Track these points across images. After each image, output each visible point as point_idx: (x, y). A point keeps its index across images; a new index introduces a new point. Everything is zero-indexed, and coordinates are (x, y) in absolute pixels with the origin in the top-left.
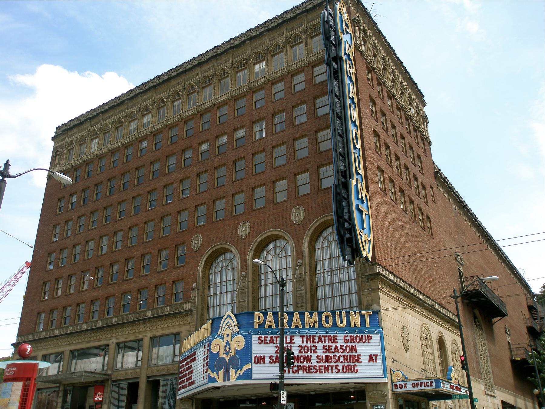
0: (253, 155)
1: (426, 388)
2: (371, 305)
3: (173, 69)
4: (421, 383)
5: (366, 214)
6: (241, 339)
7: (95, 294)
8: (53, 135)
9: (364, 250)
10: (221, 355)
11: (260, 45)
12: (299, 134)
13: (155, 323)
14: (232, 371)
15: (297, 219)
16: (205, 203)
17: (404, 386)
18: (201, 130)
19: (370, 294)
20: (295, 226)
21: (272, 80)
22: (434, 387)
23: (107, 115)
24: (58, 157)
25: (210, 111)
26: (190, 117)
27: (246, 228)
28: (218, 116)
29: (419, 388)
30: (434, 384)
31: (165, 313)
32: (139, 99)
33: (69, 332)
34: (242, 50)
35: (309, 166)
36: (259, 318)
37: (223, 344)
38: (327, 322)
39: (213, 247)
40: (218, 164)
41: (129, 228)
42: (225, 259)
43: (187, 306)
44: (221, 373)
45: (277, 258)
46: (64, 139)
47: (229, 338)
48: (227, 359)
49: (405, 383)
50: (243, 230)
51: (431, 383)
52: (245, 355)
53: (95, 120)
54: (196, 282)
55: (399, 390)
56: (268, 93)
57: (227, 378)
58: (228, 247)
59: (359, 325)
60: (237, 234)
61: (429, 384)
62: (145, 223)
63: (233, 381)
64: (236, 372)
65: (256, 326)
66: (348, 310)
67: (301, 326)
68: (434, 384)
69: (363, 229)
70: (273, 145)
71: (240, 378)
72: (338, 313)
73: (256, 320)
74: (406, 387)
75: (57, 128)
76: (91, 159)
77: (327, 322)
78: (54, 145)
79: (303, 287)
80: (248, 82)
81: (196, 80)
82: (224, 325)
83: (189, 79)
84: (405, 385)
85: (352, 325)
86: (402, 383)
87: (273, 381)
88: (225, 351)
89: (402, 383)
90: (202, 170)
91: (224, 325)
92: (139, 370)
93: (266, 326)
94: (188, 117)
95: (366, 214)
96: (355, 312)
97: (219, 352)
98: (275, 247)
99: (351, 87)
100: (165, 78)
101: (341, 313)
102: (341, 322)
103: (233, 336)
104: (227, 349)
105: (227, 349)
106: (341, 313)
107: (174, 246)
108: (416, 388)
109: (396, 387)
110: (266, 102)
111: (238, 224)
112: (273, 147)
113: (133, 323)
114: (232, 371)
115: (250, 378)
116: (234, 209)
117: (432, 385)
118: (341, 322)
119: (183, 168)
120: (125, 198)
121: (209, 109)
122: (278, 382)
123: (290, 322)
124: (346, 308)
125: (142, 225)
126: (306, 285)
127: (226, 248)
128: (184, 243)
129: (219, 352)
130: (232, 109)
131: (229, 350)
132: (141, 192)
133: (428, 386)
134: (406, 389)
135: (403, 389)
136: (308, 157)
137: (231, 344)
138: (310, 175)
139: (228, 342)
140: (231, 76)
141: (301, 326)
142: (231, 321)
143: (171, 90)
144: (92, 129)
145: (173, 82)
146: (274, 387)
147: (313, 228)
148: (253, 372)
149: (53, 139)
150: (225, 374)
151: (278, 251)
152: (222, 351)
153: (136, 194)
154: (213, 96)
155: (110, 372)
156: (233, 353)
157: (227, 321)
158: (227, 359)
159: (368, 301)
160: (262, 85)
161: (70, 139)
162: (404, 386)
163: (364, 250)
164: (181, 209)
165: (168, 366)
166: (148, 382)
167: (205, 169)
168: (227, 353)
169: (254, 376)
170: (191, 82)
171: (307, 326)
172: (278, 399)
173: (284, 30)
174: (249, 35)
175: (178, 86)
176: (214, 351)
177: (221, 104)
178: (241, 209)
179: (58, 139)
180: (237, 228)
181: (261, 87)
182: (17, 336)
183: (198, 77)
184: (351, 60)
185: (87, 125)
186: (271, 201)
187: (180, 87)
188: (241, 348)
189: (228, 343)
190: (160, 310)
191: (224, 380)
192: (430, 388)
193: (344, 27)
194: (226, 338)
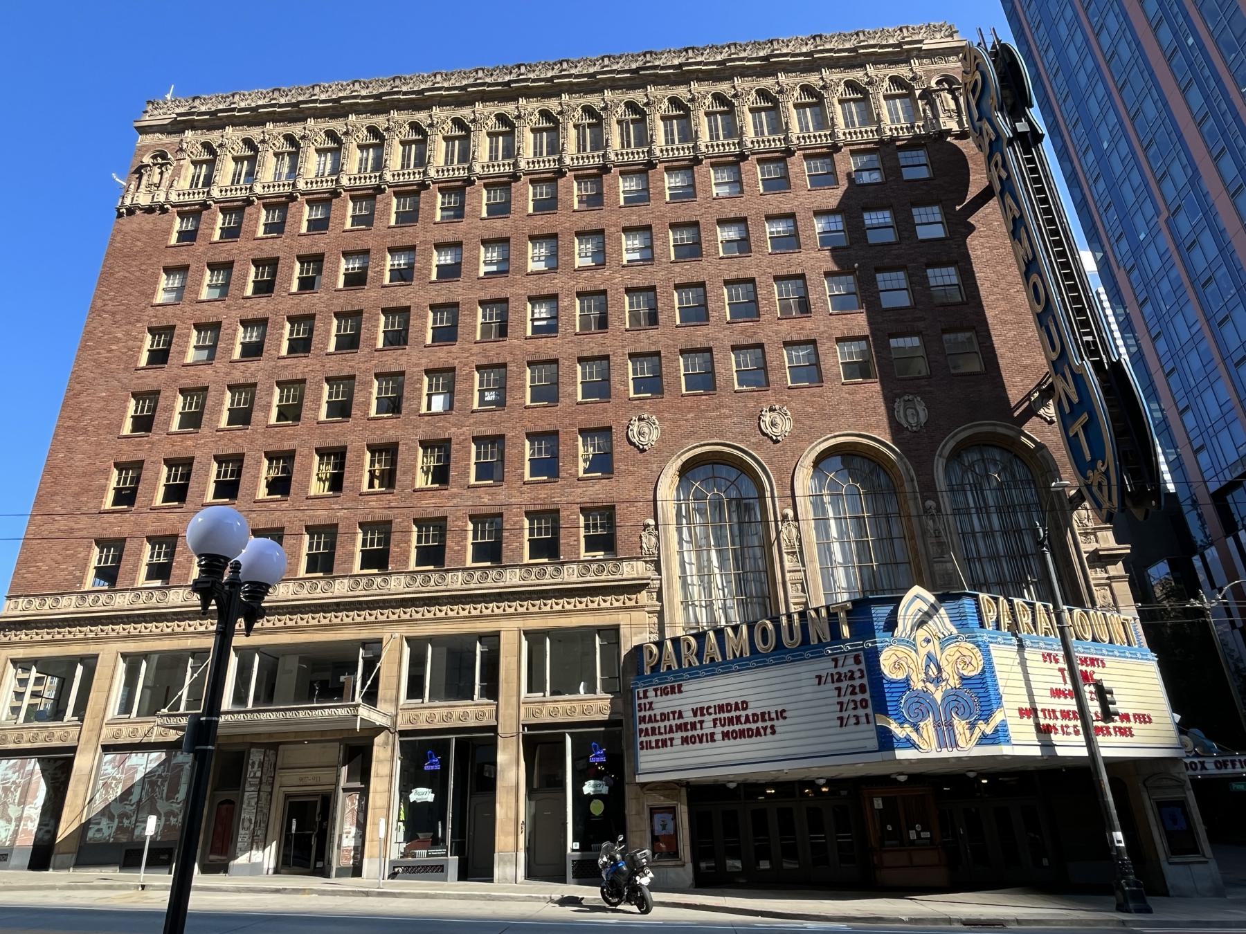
10: (918, 685)
14: (960, 725)
17: (1199, 766)
44: (928, 726)
48: (938, 696)
55: (1191, 772)
64: (972, 726)
71: (984, 740)
74: (1203, 768)
84: (1202, 763)
86: (1196, 760)
89: (1196, 760)
108: (1223, 771)
114: (960, 725)
115: (1008, 742)
139: (929, 657)
147: (952, 444)
148: (1011, 728)
156: (954, 682)
158: (938, 696)
169: (1014, 737)
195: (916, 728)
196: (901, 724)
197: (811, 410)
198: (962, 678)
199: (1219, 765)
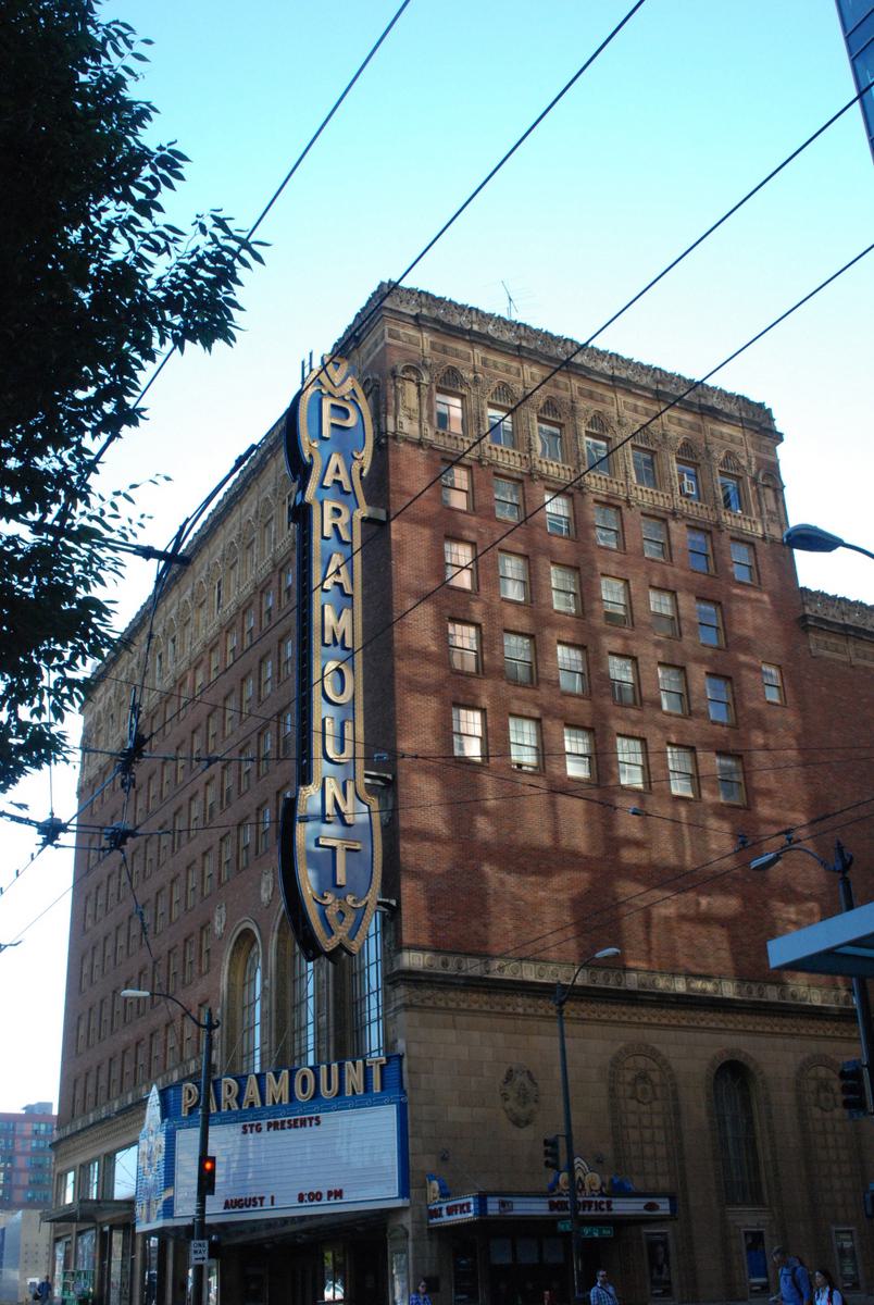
30: (472, 1207)
51: (468, 1204)
65: (185, 1114)
67: (258, 1105)
73: (185, 1094)
85: (348, 1093)
99: (337, 560)
102: (329, 1088)
108: (451, 1218)
141: (258, 1105)
148: (177, 1203)
163: (331, 932)
164: (205, 849)
171: (269, 1103)
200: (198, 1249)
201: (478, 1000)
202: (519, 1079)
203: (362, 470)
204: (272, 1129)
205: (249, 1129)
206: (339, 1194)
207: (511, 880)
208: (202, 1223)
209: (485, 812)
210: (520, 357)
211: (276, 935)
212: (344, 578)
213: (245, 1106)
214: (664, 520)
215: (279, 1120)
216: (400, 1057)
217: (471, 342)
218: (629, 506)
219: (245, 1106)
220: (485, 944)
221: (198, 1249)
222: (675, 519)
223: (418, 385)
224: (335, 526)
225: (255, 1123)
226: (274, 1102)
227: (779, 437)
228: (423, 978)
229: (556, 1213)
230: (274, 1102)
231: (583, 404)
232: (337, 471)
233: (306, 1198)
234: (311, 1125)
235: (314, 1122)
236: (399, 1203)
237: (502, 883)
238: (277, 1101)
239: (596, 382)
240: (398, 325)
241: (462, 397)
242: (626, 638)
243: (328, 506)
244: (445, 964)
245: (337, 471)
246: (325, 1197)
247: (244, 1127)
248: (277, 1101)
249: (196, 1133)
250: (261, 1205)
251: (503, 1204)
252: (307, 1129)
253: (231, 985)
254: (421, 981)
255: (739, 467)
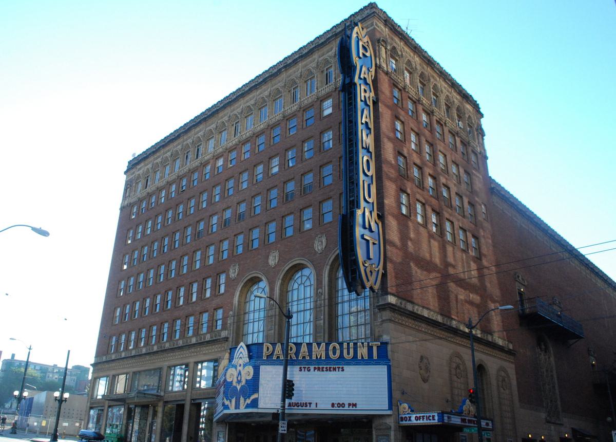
0: (284, 183)
1: (429, 421)
2: (382, 336)
3: (222, 100)
4: (423, 417)
5: (374, 244)
6: (251, 369)
7: (153, 320)
8: (125, 169)
9: (368, 280)
10: (234, 384)
11: (295, 72)
12: (325, 161)
13: (198, 349)
14: (242, 399)
15: (319, 248)
16: (242, 232)
17: (408, 419)
18: (242, 159)
19: (381, 324)
20: (318, 255)
21: (303, 107)
22: (436, 421)
23: (167, 149)
24: (128, 189)
25: (250, 140)
26: (233, 148)
27: (275, 257)
28: (257, 145)
29: (421, 422)
31: (207, 340)
32: (193, 132)
33: (132, 355)
34: (279, 78)
35: (332, 193)
36: (268, 348)
37: (236, 374)
38: (334, 353)
39: (248, 276)
40: (255, 193)
41: (181, 257)
42: (258, 288)
43: (224, 334)
45: (303, 286)
46: (134, 172)
47: (241, 368)
48: (239, 387)
49: (409, 415)
50: (273, 261)
51: (433, 416)
52: (253, 385)
53: (158, 154)
54: (232, 311)
56: (299, 120)
57: (237, 406)
58: (260, 276)
59: (366, 357)
60: (268, 263)
61: (431, 418)
62: (194, 252)
63: (242, 410)
64: (245, 400)
65: (265, 358)
66: (355, 341)
68: (436, 418)
69: (369, 258)
70: (302, 173)
71: (247, 406)
72: (345, 345)
73: (265, 349)
74: (410, 420)
75: (129, 162)
76: (153, 191)
77: (334, 353)
78: (126, 178)
79: (322, 317)
80: (283, 110)
81: (239, 110)
82: (238, 354)
83: (234, 110)
84: (410, 417)
85: (359, 357)
86: (407, 416)
87: (275, 411)
88: (238, 380)
89: (407, 416)
90: (241, 199)
91: (238, 354)
92: (185, 393)
93: (275, 358)
94: (231, 147)
95: (374, 244)
96: (363, 343)
97: (232, 381)
98: (302, 276)
99: (366, 112)
100: (214, 110)
101: (348, 344)
102: (348, 353)
103: (245, 366)
104: (239, 379)
105: (239, 379)
106: (348, 344)
107: (215, 274)
108: (419, 422)
109: (402, 419)
110: (297, 130)
111: (269, 253)
112: (302, 175)
113: (180, 348)
114: (242, 399)
116: (267, 238)
117: (434, 419)
118: (348, 353)
119: (226, 198)
120: (178, 228)
121: (249, 139)
122: (280, 411)
123: (297, 354)
124: (362, 339)
125: (191, 254)
126: (324, 315)
127: (258, 277)
128: (224, 272)
129: (232, 381)
130: (269, 138)
131: (241, 379)
132: (191, 222)
133: (430, 420)
134: (410, 422)
135: (408, 422)
136: (331, 184)
137: (242, 373)
138: (333, 203)
140: (269, 105)
142: (243, 351)
143: (219, 122)
144: (155, 162)
145: (221, 114)
146: (275, 416)
149: (125, 173)
150: (236, 402)
151: (304, 278)
152: (235, 380)
153: (187, 225)
154: (253, 126)
155: (162, 394)
156: (243, 383)
157: (239, 352)
158: (239, 387)
159: (379, 331)
160: (295, 112)
161: (138, 173)
162: (408, 419)
163: (368, 280)
164: (222, 239)
165: (208, 391)
166: (192, 404)
167: (243, 199)
168: (239, 382)
169: (260, 406)
170: (235, 112)
171: (314, 357)
172: (276, 427)
173: (316, 56)
174: (286, 63)
175: (224, 117)
176: (229, 380)
177: (259, 133)
178: (272, 238)
179: (129, 173)
180: (267, 257)
181: (294, 114)
182: (95, 357)
183: (241, 107)
184: (369, 85)
185: (152, 158)
186: (299, 229)
187: (226, 118)
188: (250, 378)
189: (240, 372)
190: (202, 337)
191: (236, 408)
192: (432, 421)
193: (361, 51)
194: (239, 368)
195: (231, 401)
196: (227, 400)
197: (286, 250)
198: (246, 380)
199: (417, 418)
200: (283, 425)
201: (410, 322)
202: (425, 361)
203: (372, 76)
204: (316, 370)
205: (303, 369)
206: (355, 405)
207: (419, 271)
208: (283, 413)
209: (411, 240)
210: (415, 52)
211: (280, 281)
212: (368, 120)
213: (301, 358)
214: (454, 135)
215: (321, 366)
216: (386, 343)
217: (401, 39)
218: (446, 126)
219: (301, 358)
220: (412, 297)
221: (283, 425)
222: (458, 136)
223: (386, 49)
224: (365, 96)
225: (307, 366)
226: (317, 357)
227: (482, 116)
228: (397, 308)
229: (463, 424)
230: (317, 357)
231: (432, 80)
232: (365, 73)
233: (336, 405)
234: (339, 371)
235: (340, 369)
236: (389, 412)
237: (416, 272)
238: (319, 357)
239: (435, 71)
240: (378, 21)
241: (396, 61)
242: (446, 179)
243: (363, 87)
244: (401, 303)
245: (365, 73)
246: (347, 406)
247: (300, 368)
248: (319, 357)
249: (280, 369)
250: (310, 407)
251: (449, 418)
252: (337, 372)
253: (239, 302)
254: (396, 310)
255: (472, 123)
